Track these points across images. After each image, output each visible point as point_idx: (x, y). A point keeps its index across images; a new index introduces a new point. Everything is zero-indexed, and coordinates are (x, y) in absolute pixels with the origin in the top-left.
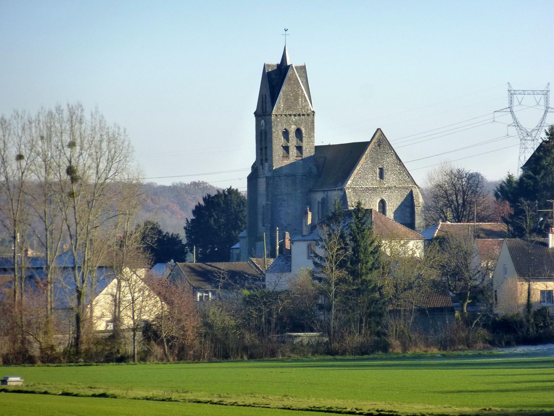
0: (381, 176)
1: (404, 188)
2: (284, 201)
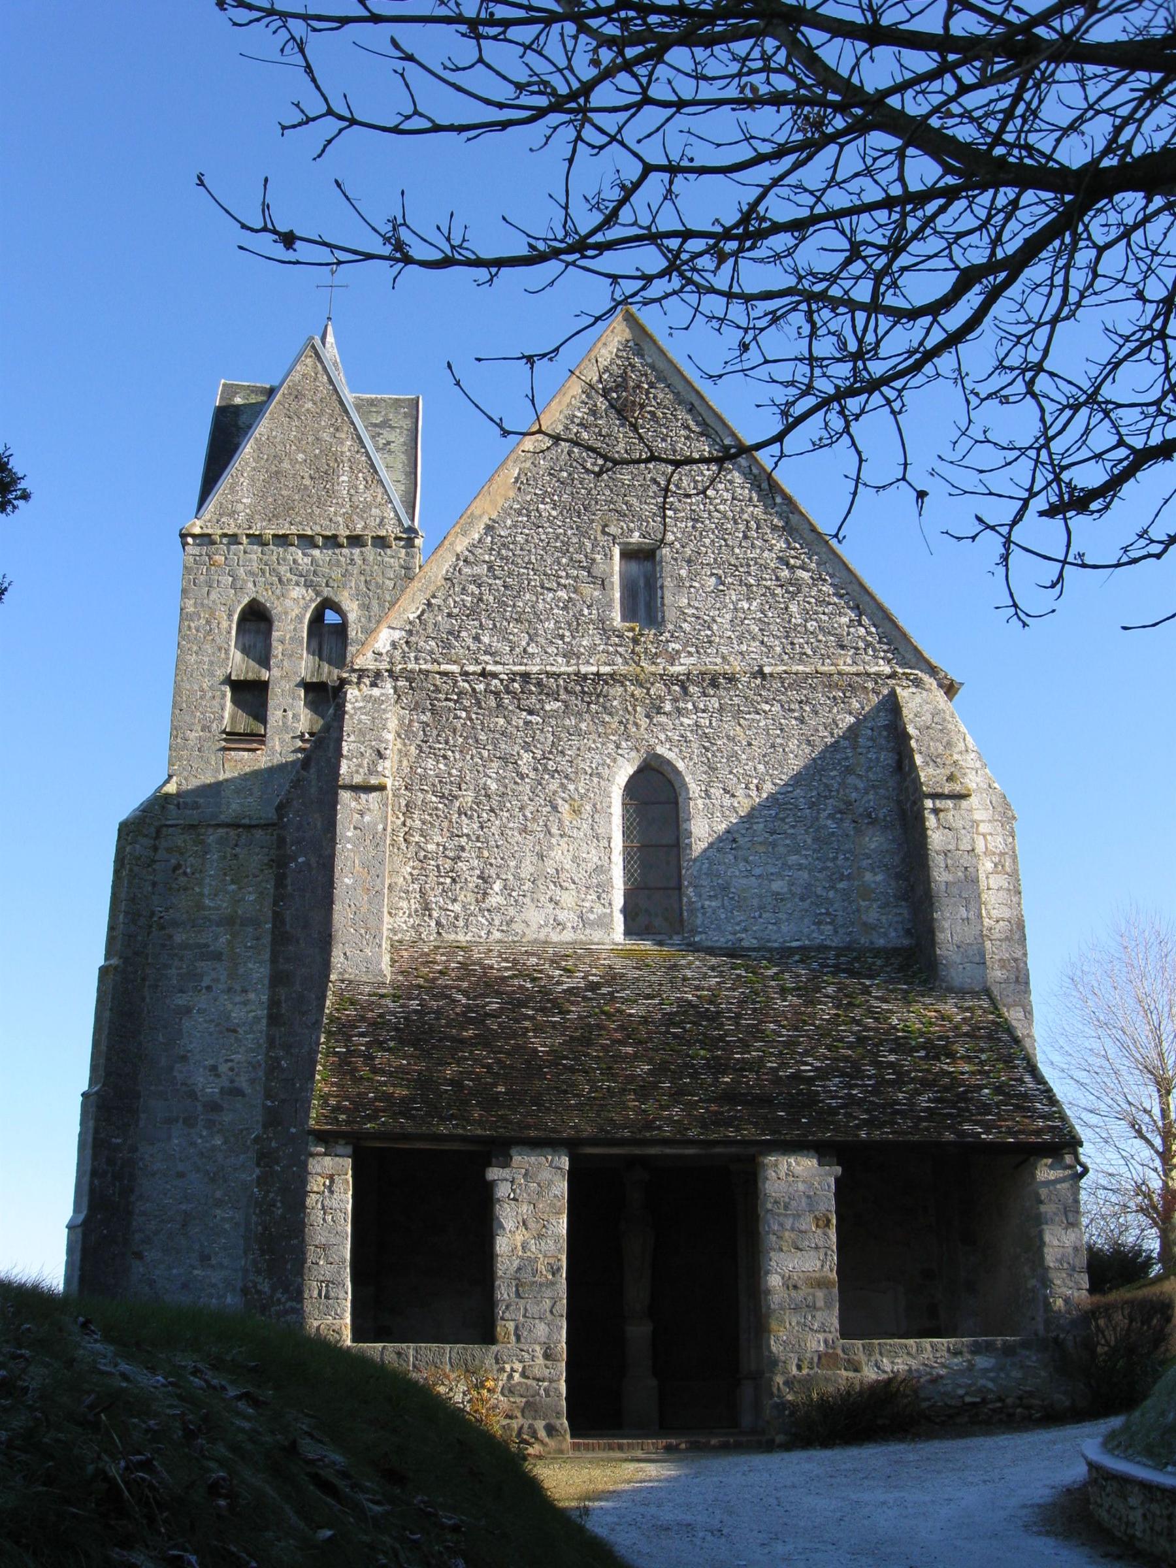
0: (644, 601)
1: (829, 681)
2: (217, 956)
